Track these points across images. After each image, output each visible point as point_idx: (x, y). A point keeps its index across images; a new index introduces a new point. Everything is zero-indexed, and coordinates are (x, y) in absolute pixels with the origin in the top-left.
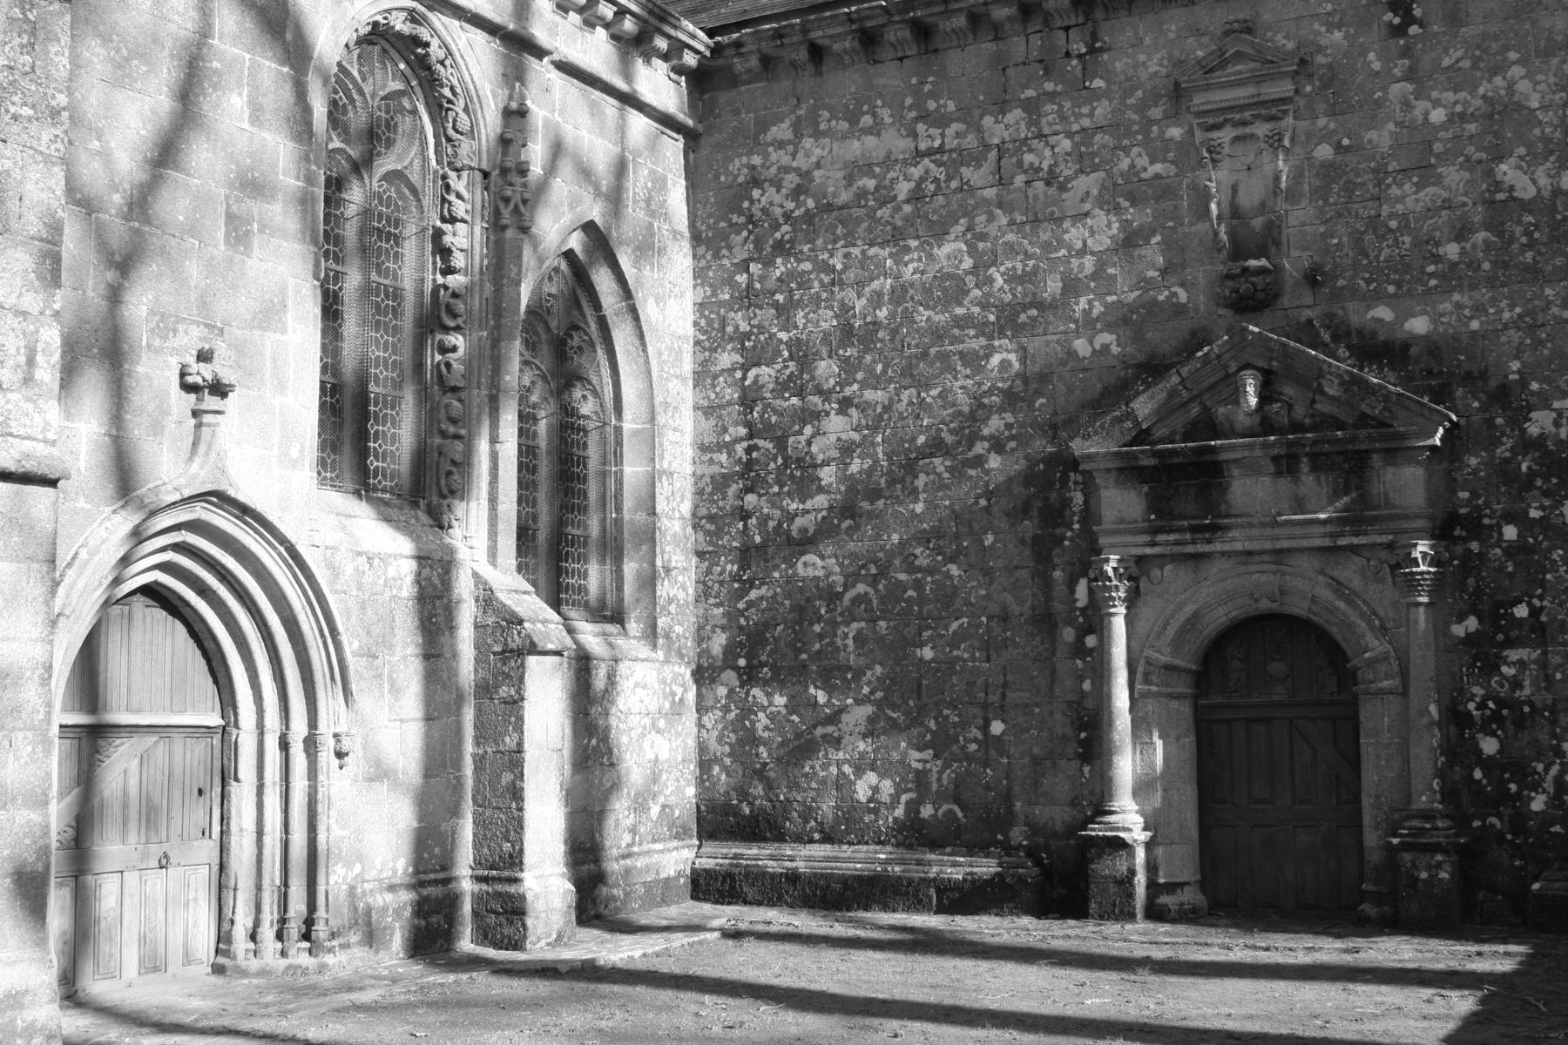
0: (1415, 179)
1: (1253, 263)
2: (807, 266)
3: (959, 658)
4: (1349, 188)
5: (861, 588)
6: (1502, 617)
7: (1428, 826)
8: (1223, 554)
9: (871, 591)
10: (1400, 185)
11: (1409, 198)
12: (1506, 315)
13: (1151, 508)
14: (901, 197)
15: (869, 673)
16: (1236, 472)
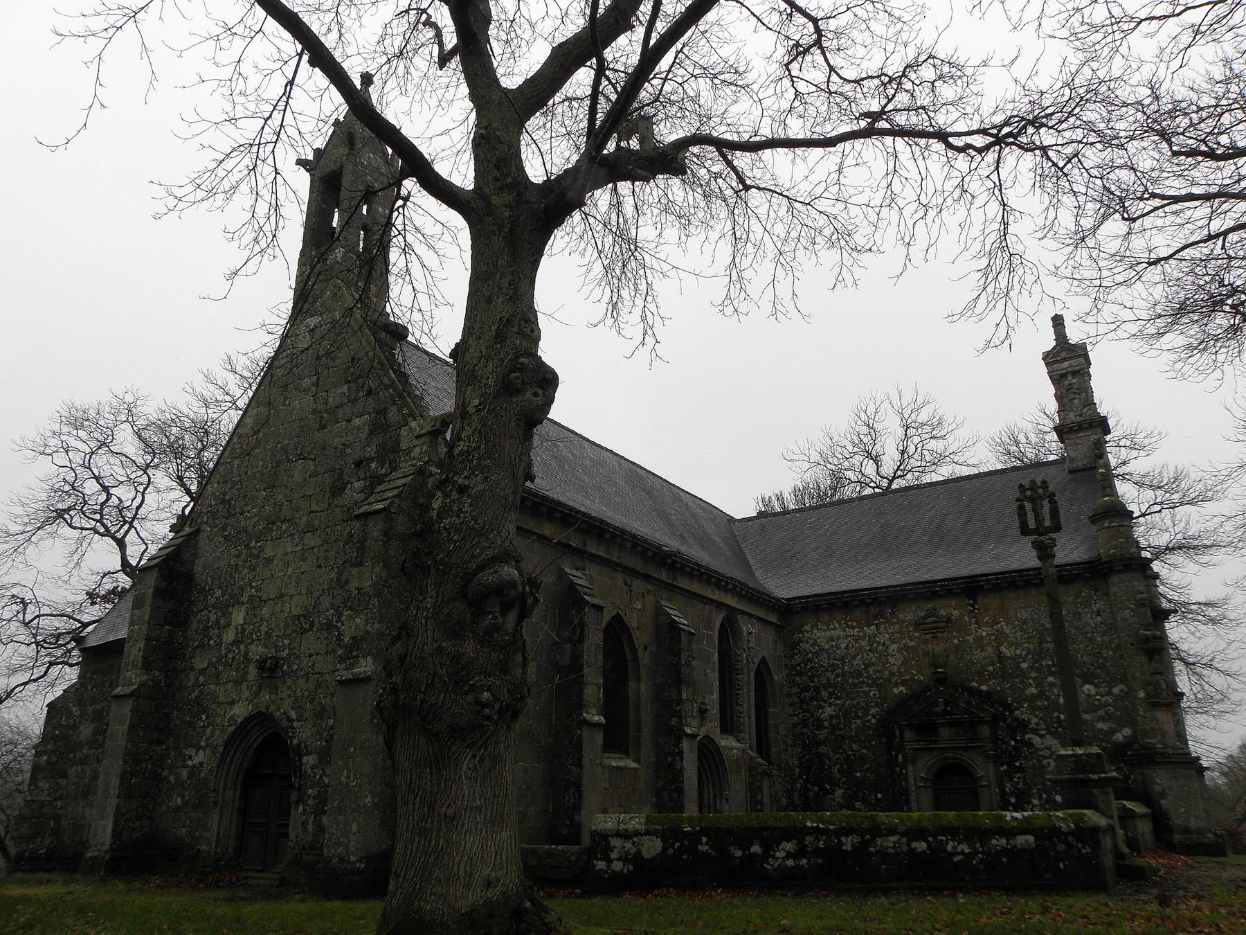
2: (817, 665)
11: (979, 654)
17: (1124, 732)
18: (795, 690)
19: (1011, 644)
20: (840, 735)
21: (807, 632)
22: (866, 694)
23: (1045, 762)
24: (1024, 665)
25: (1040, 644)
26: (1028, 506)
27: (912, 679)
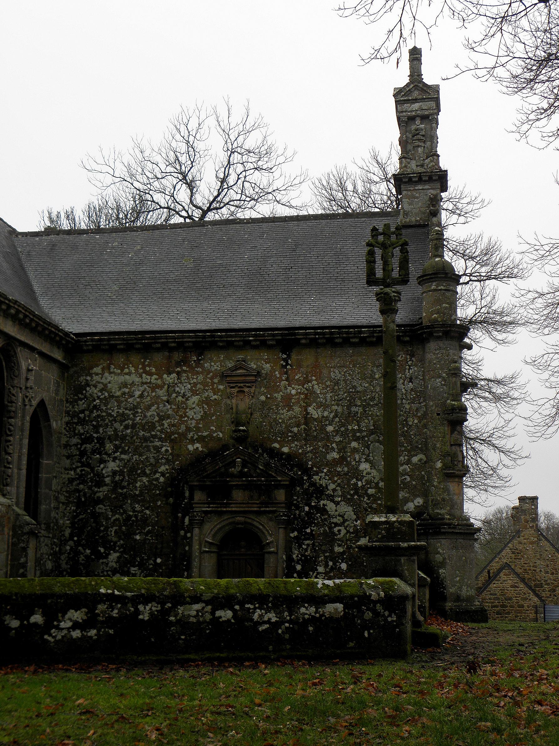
1: (241, 428)
2: (104, 414)
3: (149, 539)
4: (269, 409)
5: (117, 516)
9: (121, 518)
10: (283, 410)
11: (285, 414)
12: (309, 449)
14: (136, 396)
15: (119, 543)
17: (416, 502)
18: (75, 440)
19: (320, 405)
20: (121, 494)
21: (97, 374)
22: (157, 449)
23: (336, 530)
24: (330, 428)
25: (349, 407)
26: (378, 252)
27: (210, 436)
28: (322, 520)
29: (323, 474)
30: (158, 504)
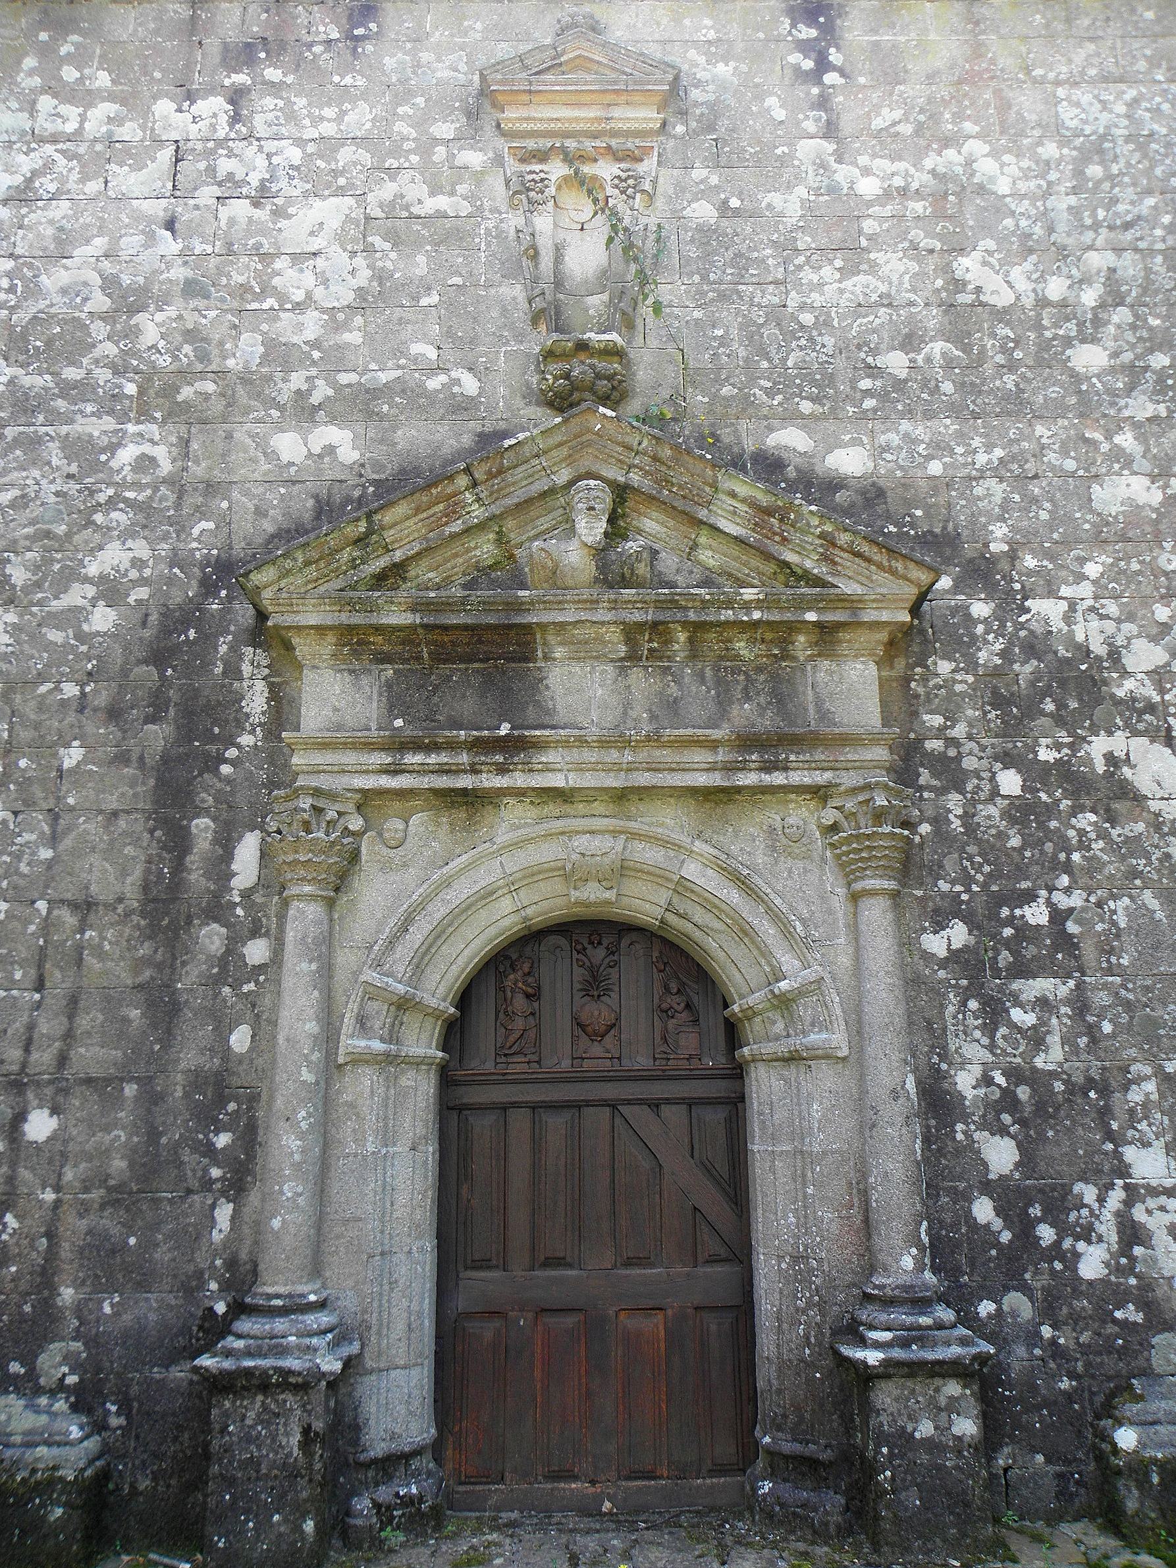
0: (838, 263)
6: (1010, 921)
7: (924, 1320)
8: (520, 793)
12: (982, 459)
13: (395, 703)
16: (559, 652)
28: (1112, 847)
29: (1085, 590)
30: (68, 764)
